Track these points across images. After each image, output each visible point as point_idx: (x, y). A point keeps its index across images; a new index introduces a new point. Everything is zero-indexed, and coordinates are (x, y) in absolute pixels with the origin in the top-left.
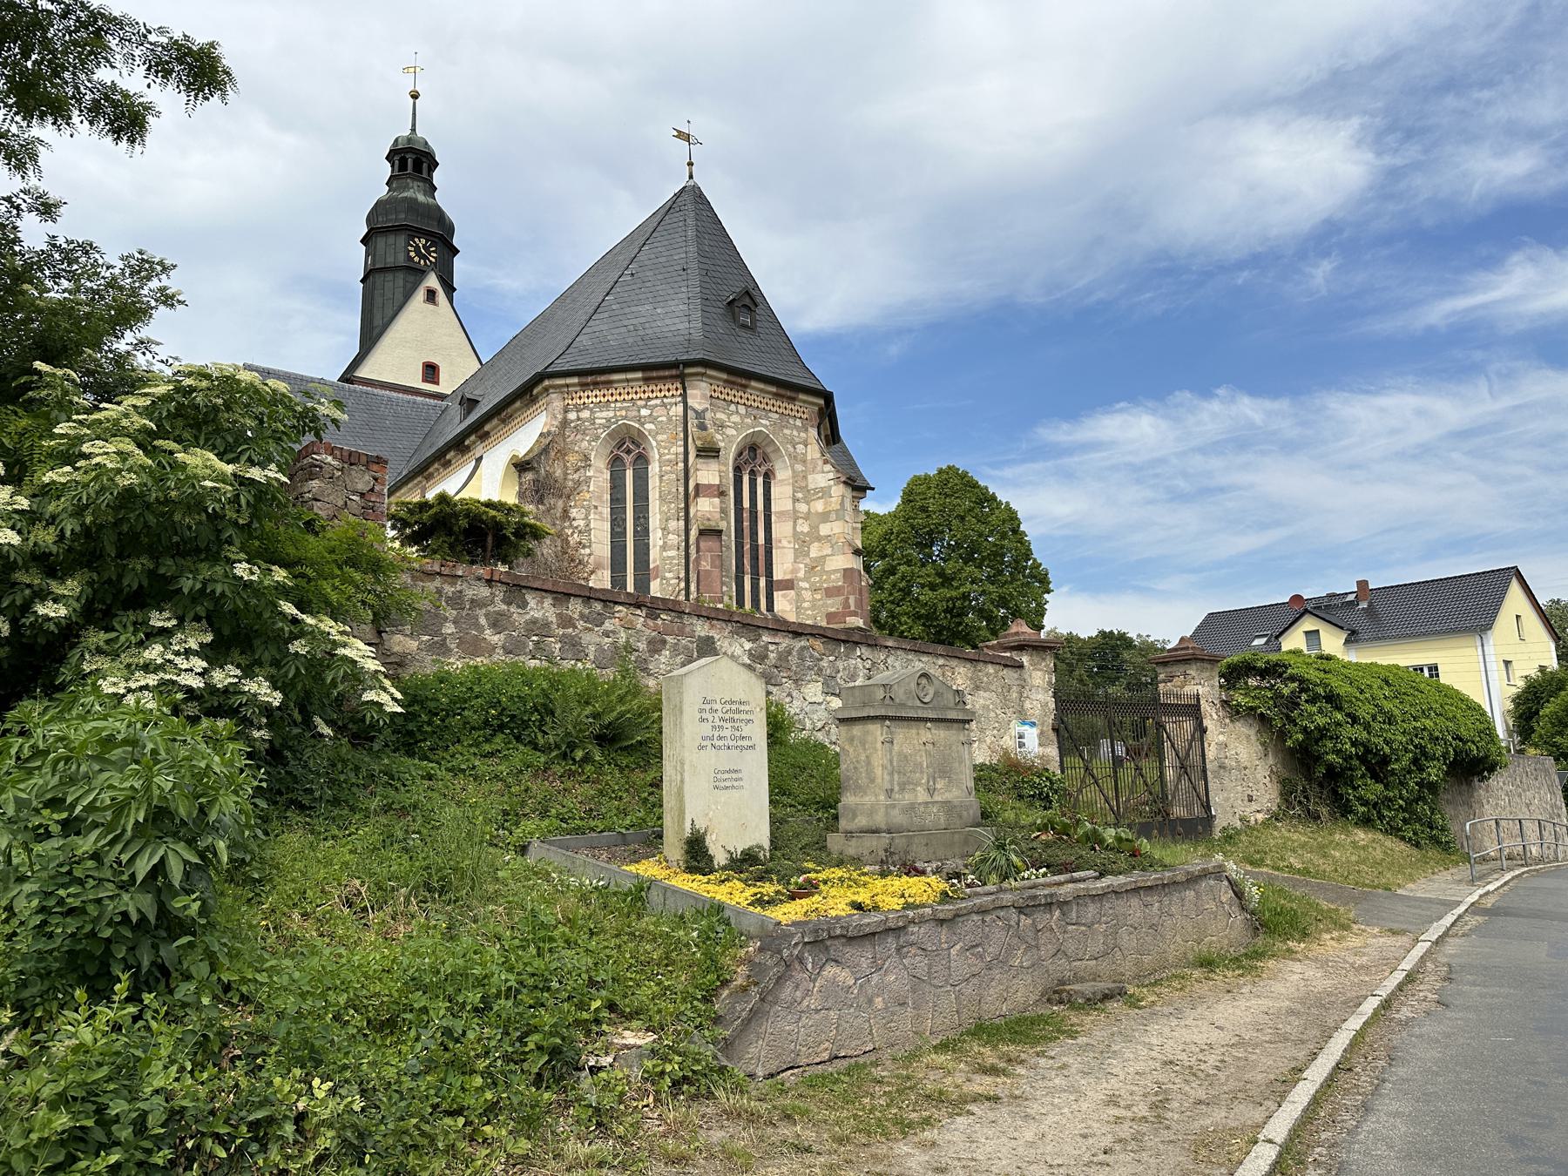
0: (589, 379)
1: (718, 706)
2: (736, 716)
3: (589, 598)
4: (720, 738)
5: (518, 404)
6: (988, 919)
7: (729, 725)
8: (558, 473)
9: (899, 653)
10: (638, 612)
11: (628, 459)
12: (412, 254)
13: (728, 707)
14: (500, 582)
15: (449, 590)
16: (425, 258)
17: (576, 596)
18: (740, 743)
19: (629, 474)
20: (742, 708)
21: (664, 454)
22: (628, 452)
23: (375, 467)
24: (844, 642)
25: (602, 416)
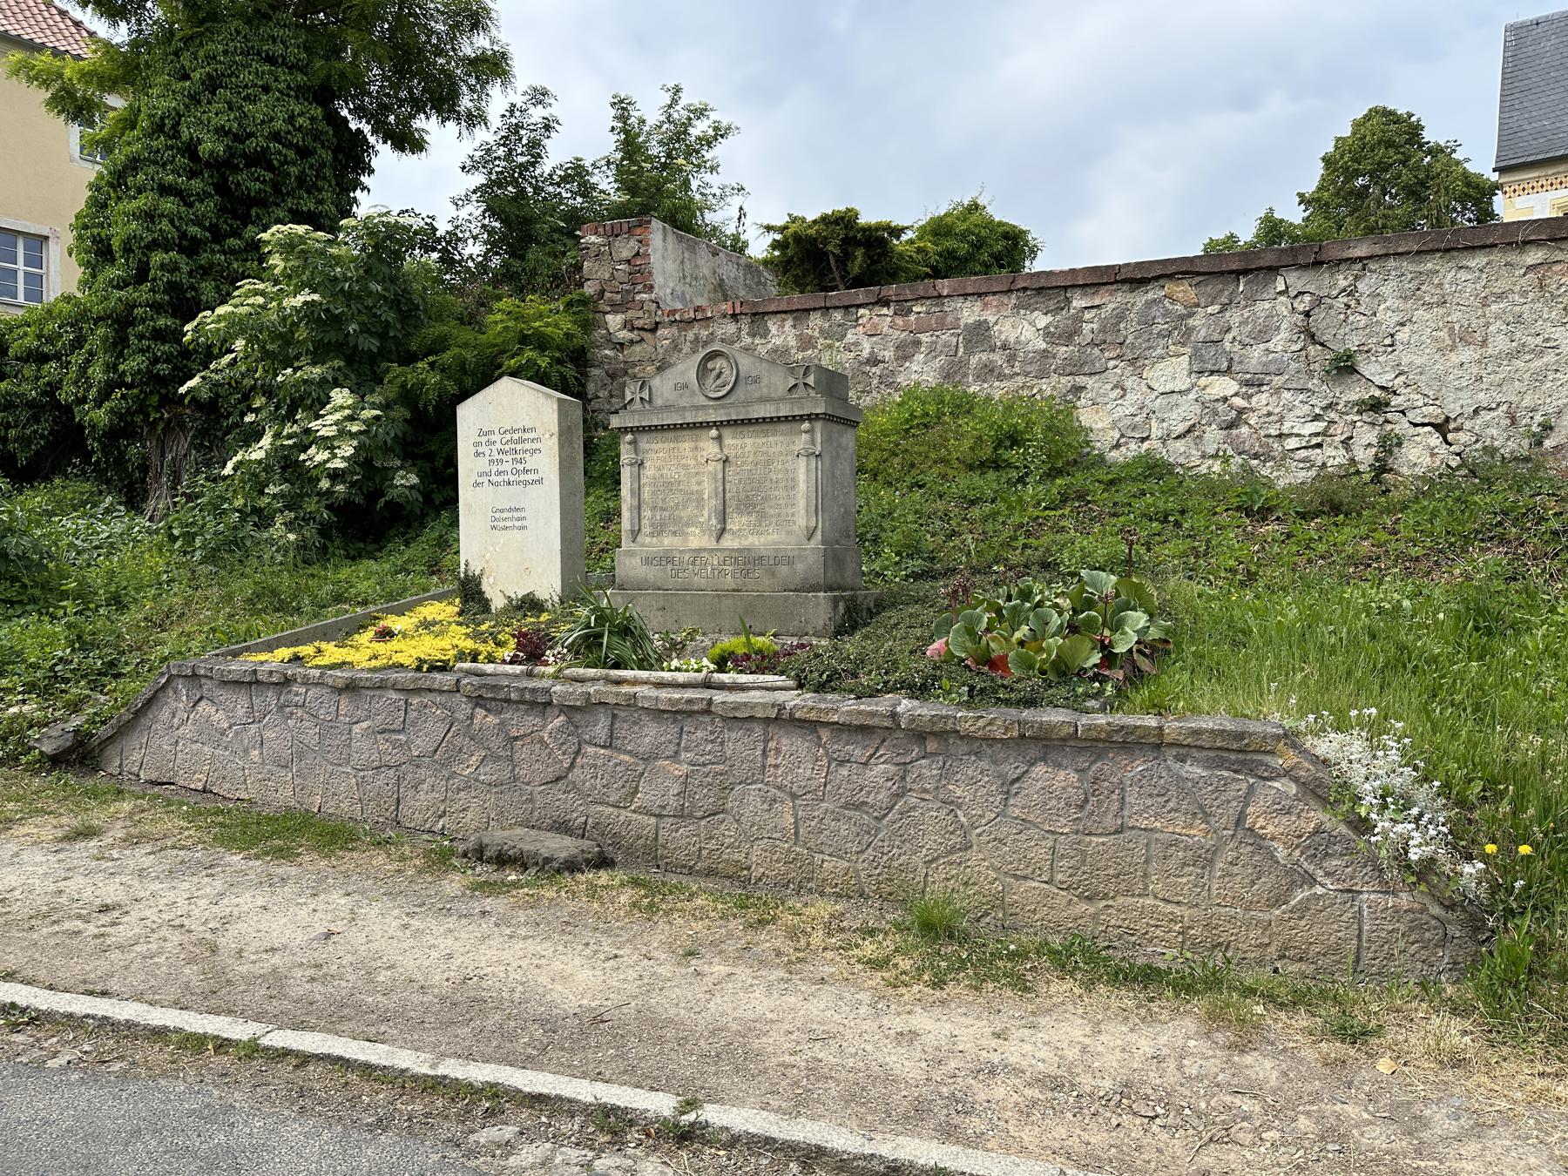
1: (496, 437)
2: (519, 447)
3: (828, 309)
4: (499, 473)
6: (415, 701)
7: (509, 458)
9: (1391, 263)
10: (885, 311)
13: (508, 437)
15: (704, 333)
17: (815, 309)
18: (523, 477)
20: (526, 436)
23: (638, 231)
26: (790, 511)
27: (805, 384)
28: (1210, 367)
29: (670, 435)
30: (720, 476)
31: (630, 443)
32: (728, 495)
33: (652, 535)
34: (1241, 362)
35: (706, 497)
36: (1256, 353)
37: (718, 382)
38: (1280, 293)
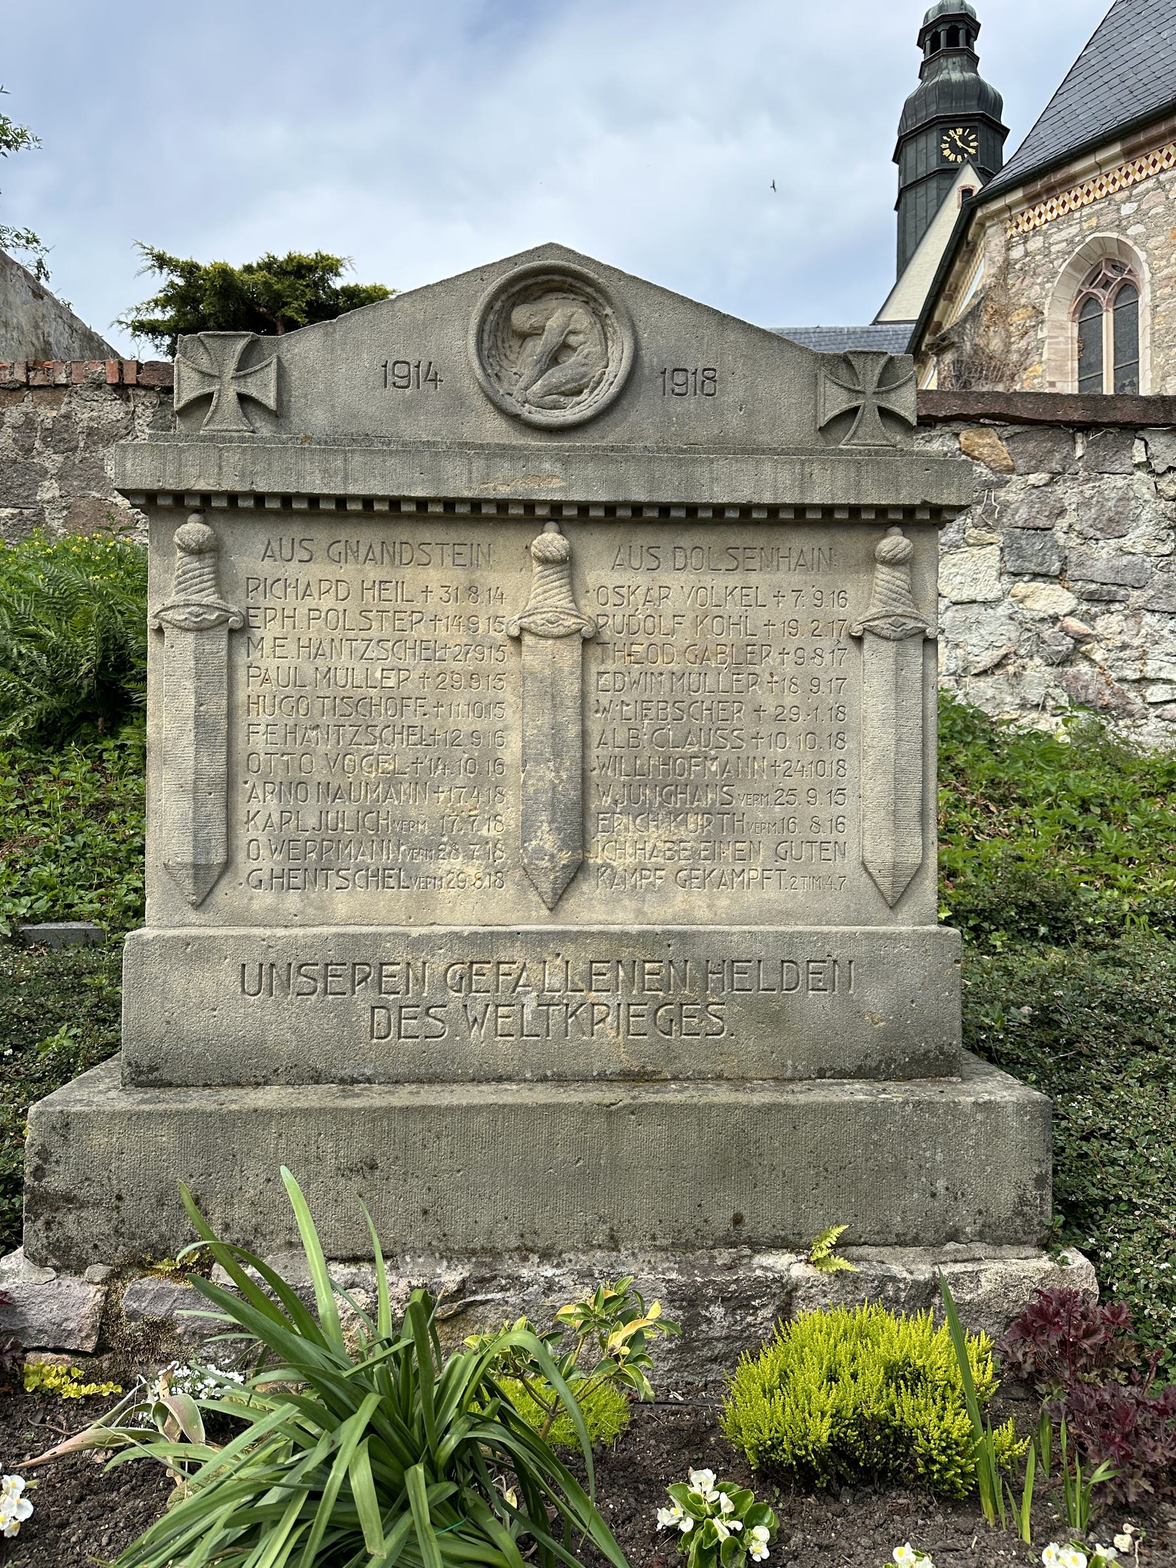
0: (1039, 185)
5: (958, 265)
8: (996, 344)
11: (1104, 296)
12: (947, 153)
14: (138, 385)
15: (48, 415)
16: (962, 151)
19: (1108, 319)
21: (1160, 269)
22: (1106, 284)
24: (1085, 427)
25: (1060, 238)
26: (824, 810)
27: (885, 413)
28: (1033, 567)
29: (369, 536)
30: (571, 688)
31: (197, 552)
32: (595, 752)
33: (281, 881)
34: (1080, 565)
35: (511, 751)
36: (1103, 553)
37: (556, 376)
38: (1137, 466)
